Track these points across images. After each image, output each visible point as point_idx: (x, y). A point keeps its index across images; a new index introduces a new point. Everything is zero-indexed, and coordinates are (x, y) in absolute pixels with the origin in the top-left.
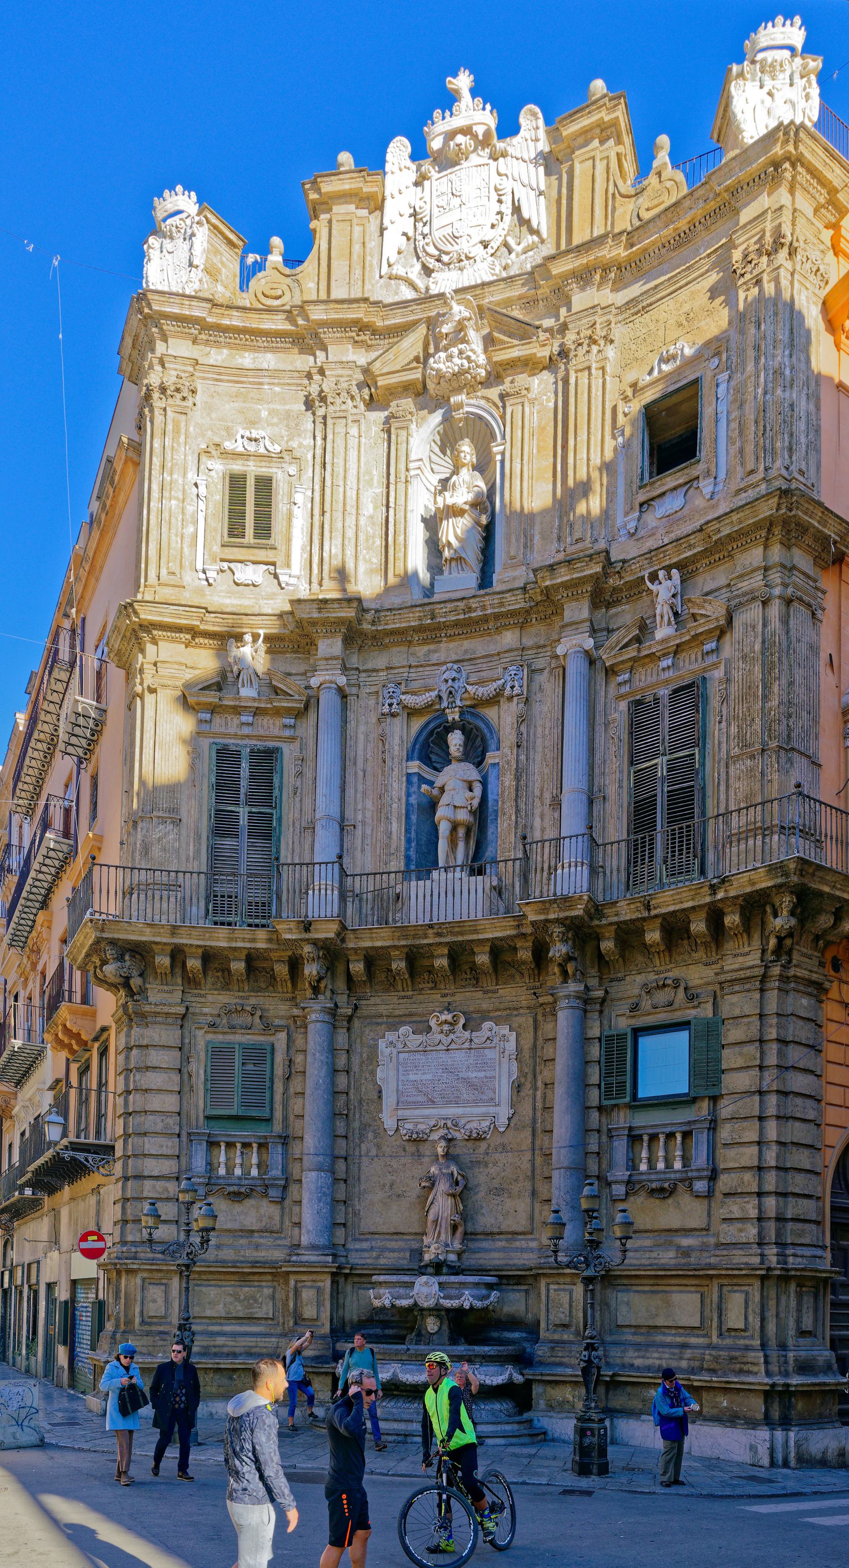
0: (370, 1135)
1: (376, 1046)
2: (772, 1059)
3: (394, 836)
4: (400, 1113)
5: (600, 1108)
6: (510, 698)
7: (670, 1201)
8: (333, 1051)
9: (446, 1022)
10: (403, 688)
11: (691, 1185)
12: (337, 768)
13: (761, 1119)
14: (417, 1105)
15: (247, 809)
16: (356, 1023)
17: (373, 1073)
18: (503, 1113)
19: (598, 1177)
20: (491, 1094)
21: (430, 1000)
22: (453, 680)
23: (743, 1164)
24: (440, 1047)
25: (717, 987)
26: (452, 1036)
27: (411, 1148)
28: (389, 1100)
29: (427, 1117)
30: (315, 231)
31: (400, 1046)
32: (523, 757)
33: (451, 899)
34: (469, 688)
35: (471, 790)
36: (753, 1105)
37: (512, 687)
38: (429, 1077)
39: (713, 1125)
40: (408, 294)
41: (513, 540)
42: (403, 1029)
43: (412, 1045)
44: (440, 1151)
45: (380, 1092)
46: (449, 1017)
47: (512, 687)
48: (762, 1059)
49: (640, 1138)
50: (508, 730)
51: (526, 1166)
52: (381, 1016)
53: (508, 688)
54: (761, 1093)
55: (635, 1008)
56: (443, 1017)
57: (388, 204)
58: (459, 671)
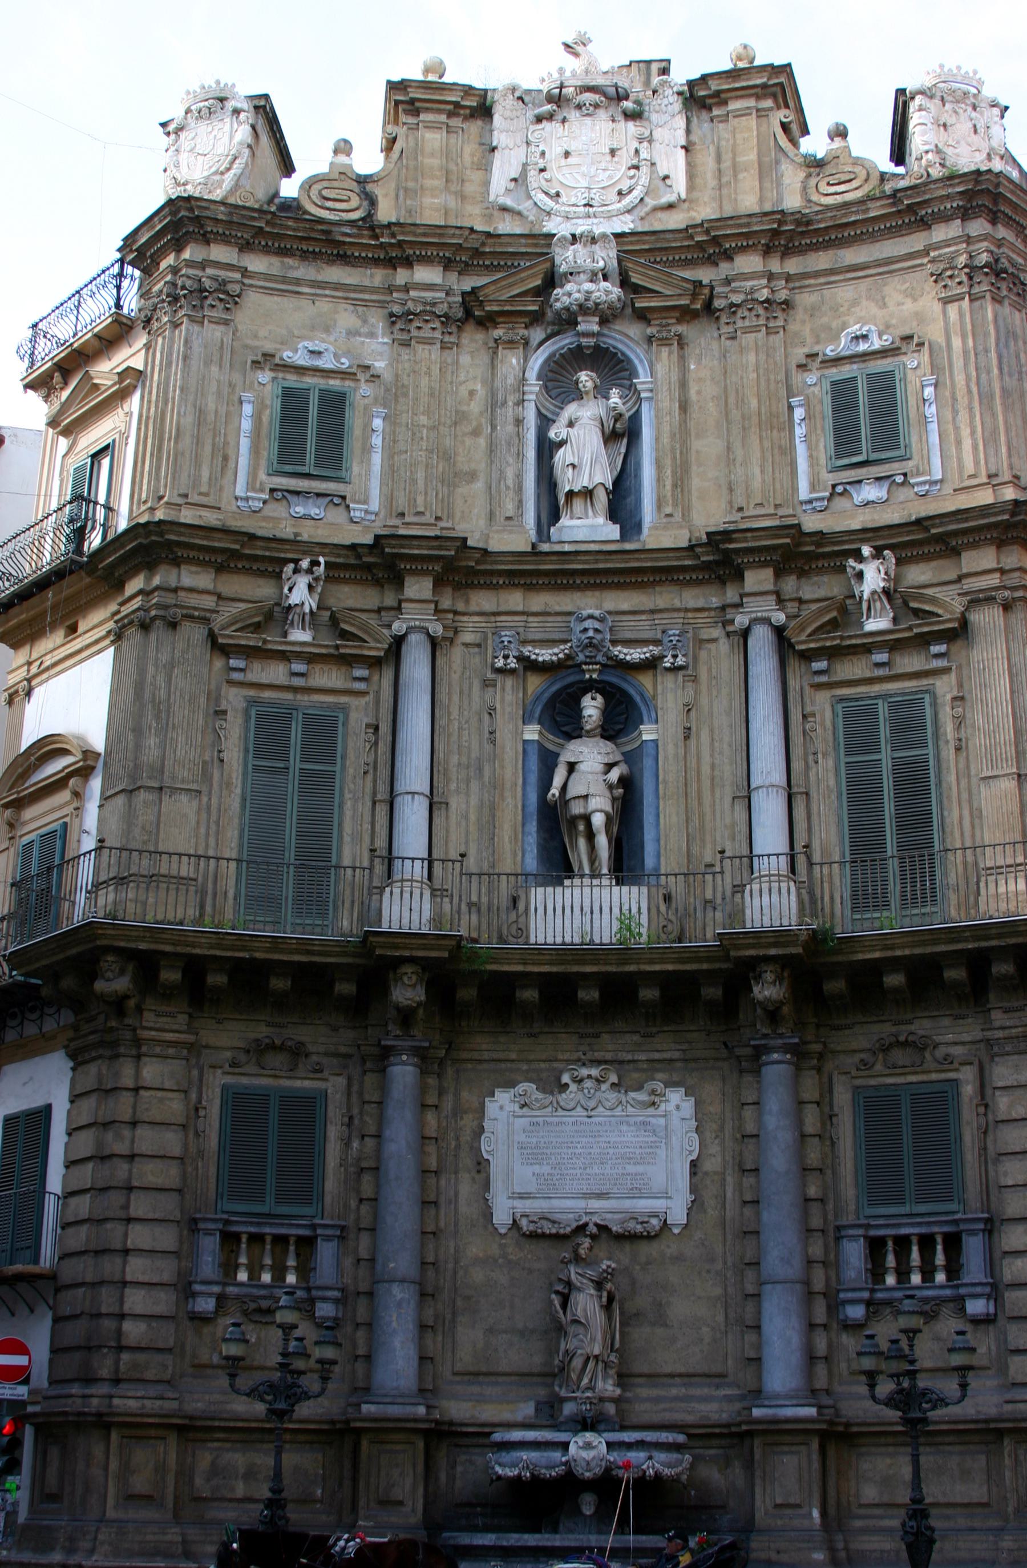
11: (963, 1309)
19: (824, 1294)
47: (675, 656)
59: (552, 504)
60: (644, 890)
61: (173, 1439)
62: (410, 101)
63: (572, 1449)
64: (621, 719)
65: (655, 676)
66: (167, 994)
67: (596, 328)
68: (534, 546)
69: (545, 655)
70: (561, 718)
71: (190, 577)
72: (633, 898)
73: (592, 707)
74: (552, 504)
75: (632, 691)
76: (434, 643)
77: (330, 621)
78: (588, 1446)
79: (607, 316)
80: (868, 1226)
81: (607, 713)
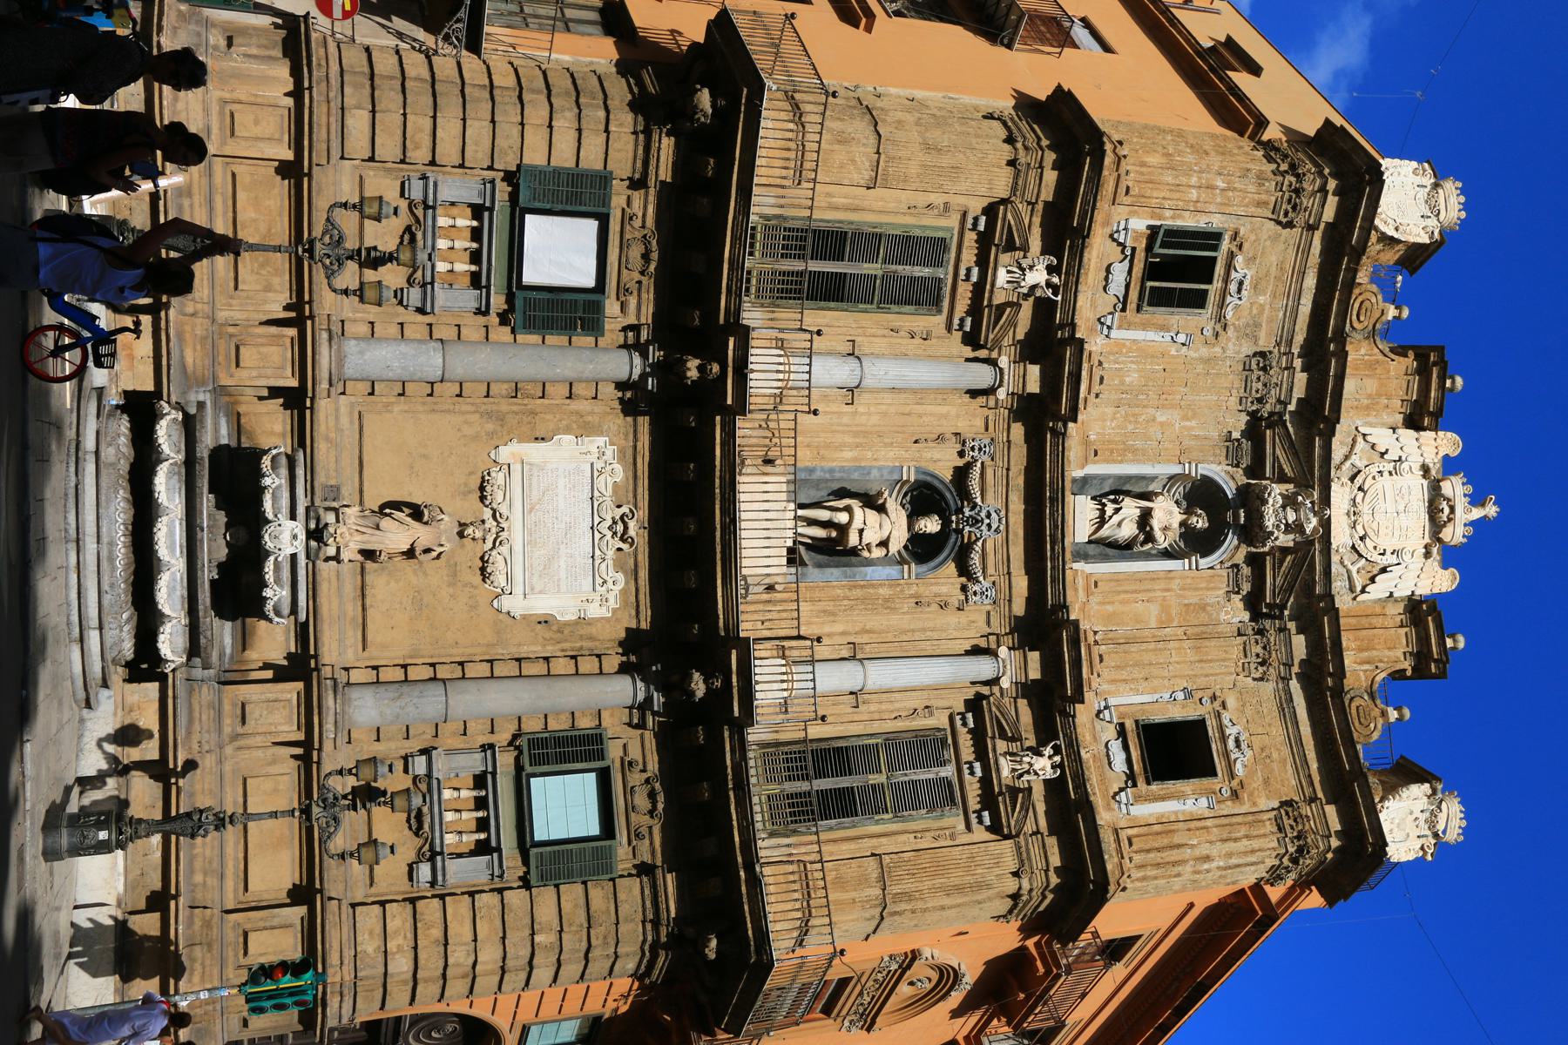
0: (490, 427)
1: (601, 434)
4: (518, 466)
6: (964, 589)
9: (626, 528)
10: (988, 462)
12: (914, 385)
15: (880, 273)
17: (567, 431)
20: (538, 588)
22: (989, 526)
26: (609, 534)
28: (533, 451)
30: (1406, 356)
31: (598, 465)
33: (764, 521)
40: (1337, 456)
42: (618, 468)
43: (600, 483)
46: (632, 532)
50: (935, 589)
57: (1411, 433)
58: (997, 531)
63: (289, 525)
64: (922, 549)
70: (923, 498)
72: (777, 564)
73: (931, 525)
76: (990, 391)
78: (295, 537)
79: (1252, 532)
80: (494, 774)
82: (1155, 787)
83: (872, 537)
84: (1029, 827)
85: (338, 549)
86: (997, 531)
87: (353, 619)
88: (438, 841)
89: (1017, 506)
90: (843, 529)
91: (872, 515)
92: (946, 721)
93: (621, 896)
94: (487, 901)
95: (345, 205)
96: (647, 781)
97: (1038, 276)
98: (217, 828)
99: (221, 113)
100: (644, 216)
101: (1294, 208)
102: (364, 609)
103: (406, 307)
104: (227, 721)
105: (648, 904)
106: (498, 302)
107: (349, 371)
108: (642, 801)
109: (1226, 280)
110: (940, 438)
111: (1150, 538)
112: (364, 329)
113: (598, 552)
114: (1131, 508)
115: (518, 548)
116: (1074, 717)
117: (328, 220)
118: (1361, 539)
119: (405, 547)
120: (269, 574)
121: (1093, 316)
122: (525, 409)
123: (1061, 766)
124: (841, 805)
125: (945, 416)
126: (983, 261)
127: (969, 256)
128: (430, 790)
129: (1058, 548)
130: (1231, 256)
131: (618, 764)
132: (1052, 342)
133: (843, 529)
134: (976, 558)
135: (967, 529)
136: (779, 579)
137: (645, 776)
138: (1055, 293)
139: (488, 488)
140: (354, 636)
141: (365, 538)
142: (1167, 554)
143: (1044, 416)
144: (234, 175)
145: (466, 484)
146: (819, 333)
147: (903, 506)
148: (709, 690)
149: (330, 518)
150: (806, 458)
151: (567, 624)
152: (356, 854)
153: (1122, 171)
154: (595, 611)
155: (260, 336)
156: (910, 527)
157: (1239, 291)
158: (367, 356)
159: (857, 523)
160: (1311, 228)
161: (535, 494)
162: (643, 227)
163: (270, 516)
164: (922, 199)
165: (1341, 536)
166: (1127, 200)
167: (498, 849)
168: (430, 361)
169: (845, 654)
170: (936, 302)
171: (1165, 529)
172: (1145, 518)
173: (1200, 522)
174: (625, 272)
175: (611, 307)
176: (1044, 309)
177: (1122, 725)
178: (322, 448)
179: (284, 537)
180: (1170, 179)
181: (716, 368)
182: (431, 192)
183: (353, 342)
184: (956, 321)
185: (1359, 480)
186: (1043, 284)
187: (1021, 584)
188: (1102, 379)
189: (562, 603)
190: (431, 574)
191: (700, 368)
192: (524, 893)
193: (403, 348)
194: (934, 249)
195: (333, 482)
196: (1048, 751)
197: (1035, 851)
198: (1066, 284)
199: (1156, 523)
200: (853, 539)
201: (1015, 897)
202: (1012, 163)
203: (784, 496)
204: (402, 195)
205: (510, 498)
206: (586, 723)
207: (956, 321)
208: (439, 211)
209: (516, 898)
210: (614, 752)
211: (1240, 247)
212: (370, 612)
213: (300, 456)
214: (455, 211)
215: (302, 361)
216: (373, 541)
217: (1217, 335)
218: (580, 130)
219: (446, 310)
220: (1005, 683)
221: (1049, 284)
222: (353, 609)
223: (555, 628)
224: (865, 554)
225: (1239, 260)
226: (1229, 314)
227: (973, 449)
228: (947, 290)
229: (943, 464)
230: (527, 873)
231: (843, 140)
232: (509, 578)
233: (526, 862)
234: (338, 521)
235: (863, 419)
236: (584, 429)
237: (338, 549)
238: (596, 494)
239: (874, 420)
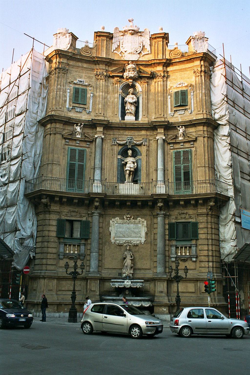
0: (107, 244)
1: (110, 222)
2: (210, 232)
3: (115, 173)
4: (115, 238)
5: (168, 240)
6: (144, 145)
7: (187, 262)
8: (99, 222)
9: (128, 217)
12: (101, 155)
13: (208, 245)
14: (120, 237)
16: (104, 216)
17: (109, 228)
18: (143, 240)
20: (140, 235)
21: (124, 211)
22: (130, 140)
23: (204, 255)
24: (127, 223)
25: (196, 215)
27: (119, 247)
28: (113, 235)
29: (123, 240)
31: (116, 222)
32: (147, 159)
33: (128, 189)
34: (134, 142)
35: (134, 164)
36: (206, 242)
37: (145, 143)
38: (124, 230)
39: (196, 246)
41: (144, 112)
44: (128, 248)
45: (110, 233)
46: (129, 216)
47: (145, 143)
48: (208, 232)
49: (178, 247)
51: (149, 253)
52: (111, 214)
53: (144, 143)
54: (208, 239)
55: (176, 218)
56: (128, 216)
57: (113, 39)
59: (124, 114)
60: (138, 185)
61: (55, 281)
62: (98, 35)
63: (125, 283)
65: (141, 147)
66: (56, 202)
67: (132, 81)
68: (120, 121)
69: (122, 143)
71: (58, 125)
72: (137, 186)
73: (130, 152)
74: (124, 114)
75: (136, 149)
77: (83, 134)
81: (132, 153)
82: (189, 104)
83: (132, 165)
84: (194, 134)
85: (130, 274)
86: (132, 138)
87: (144, 271)
88: (188, 257)
89: (127, 133)
90: (130, 171)
91: (128, 165)
92: (172, 151)
93: (201, 221)
94: (200, 247)
95: (67, 271)
96: (180, 215)
97: (78, 129)
98: (180, 297)
99: (48, 292)
100: (66, 212)
101: (64, 69)
102: (143, 269)
103: (84, 259)
104: (162, 295)
105: (203, 216)
106: (83, 242)
107: (96, 270)
108: (183, 216)
109: (79, 85)
110: (112, 150)
111: (135, 102)
112: (88, 268)
113: (133, 223)
114: (128, 106)
115: (132, 239)
116: (172, 123)
117: (69, 274)
118: (137, 52)
119: (130, 261)
120: (135, 287)
121: (87, 115)
122: (104, 236)
123: (182, 126)
124: (187, 175)
125: (107, 148)
126: (75, 140)
127: (74, 143)
128: (179, 258)
129: (136, 124)
130: (75, 84)
131: (176, 221)
132: (92, 125)
133: (130, 171)
134: (138, 143)
135: (131, 144)
136: (140, 186)
137: (178, 215)
138: (82, 124)
139: (120, 244)
140: (147, 271)
141: (129, 268)
142: (138, 98)
143: (108, 127)
144: (59, 290)
145: (119, 249)
146: (90, 178)
147: (126, 158)
148: (161, 202)
149: (124, 275)
150: (115, 180)
151: (147, 229)
152: (186, 273)
153: (56, 109)
154: (145, 223)
155: (89, 287)
156: (131, 157)
157: (82, 81)
158: (93, 267)
159: (129, 169)
160: (68, 65)
161: (121, 235)
162: (68, 212)
163: (123, 286)
164: (62, 154)
165: (135, 57)
166: (63, 108)
167: (191, 245)
168: (94, 255)
169: (156, 172)
170: (83, 151)
171: (133, 98)
172: (131, 104)
173: (131, 90)
174: (77, 216)
175: (84, 219)
176: (85, 126)
177: (174, 111)
178: (111, 276)
179: (128, 283)
180: (58, 98)
181: (97, 199)
182: (62, 254)
183: (91, 270)
184: (87, 146)
185: (123, 52)
186: (80, 127)
187: (143, 132)
188: (100, 113)
189: (143, 231)
190: (137, 255)
191: (97, 202)
192: (200, 240)
193: (92, 260)
194: (73, 151)
195: (118, 274)
196: (179, 128)
197: (200, 133)
198: (80, 122)
199: (131, 101)
200: (132, 169)
201: (208, 138)
202: (55, 134)
203: (123, 184)
204: (62, 259)
205: (122, 240)
206: (167, 227)
207: (87, 146)
208: (65, 252)
209: (200, 242)
210: (174, 221)
211: (72, 82)
212: (143, 268)
213: (113, 280)
214: (65, 249)
215: (95, 279)
216: (129, 267)
217: (91, 86)
218: (49, 225)
219: (85, 251)
220: (164, 138)
221: (80, 126)
222: (142, 271)
223: (148, 232)
224: (136, 167)
225: (75, 82)
226: (86, 84)
227: (114, 143)
228: (81, 148)
229: (117, 149)
230: (195, 239)
231: (51, 172)
232: (138, 240)
233: (194, 239)
234: (125, 274)
235: (108, 166)
236: (109, 224)
237: (130, 274)
238: (121, 223)
239: (108, 164)
